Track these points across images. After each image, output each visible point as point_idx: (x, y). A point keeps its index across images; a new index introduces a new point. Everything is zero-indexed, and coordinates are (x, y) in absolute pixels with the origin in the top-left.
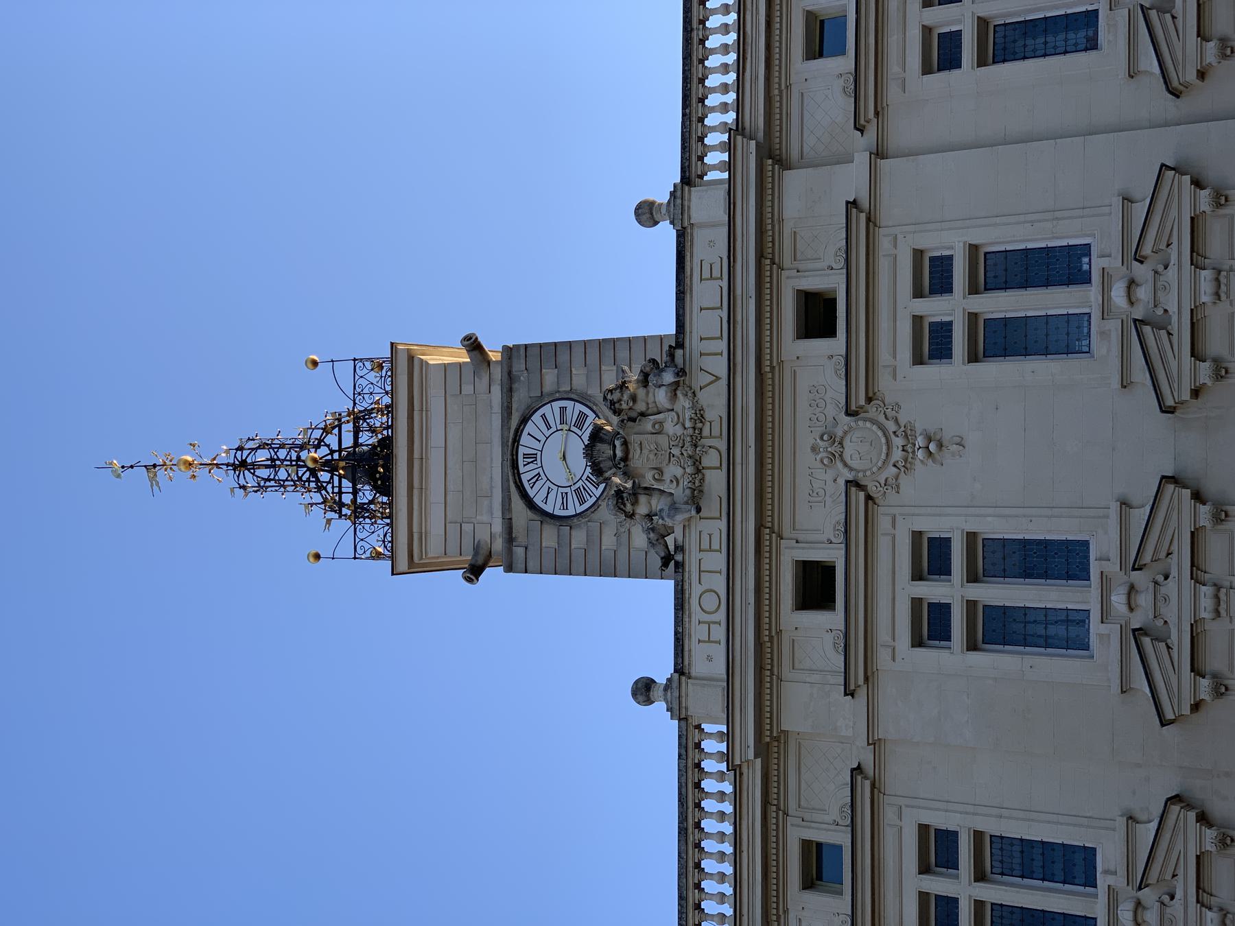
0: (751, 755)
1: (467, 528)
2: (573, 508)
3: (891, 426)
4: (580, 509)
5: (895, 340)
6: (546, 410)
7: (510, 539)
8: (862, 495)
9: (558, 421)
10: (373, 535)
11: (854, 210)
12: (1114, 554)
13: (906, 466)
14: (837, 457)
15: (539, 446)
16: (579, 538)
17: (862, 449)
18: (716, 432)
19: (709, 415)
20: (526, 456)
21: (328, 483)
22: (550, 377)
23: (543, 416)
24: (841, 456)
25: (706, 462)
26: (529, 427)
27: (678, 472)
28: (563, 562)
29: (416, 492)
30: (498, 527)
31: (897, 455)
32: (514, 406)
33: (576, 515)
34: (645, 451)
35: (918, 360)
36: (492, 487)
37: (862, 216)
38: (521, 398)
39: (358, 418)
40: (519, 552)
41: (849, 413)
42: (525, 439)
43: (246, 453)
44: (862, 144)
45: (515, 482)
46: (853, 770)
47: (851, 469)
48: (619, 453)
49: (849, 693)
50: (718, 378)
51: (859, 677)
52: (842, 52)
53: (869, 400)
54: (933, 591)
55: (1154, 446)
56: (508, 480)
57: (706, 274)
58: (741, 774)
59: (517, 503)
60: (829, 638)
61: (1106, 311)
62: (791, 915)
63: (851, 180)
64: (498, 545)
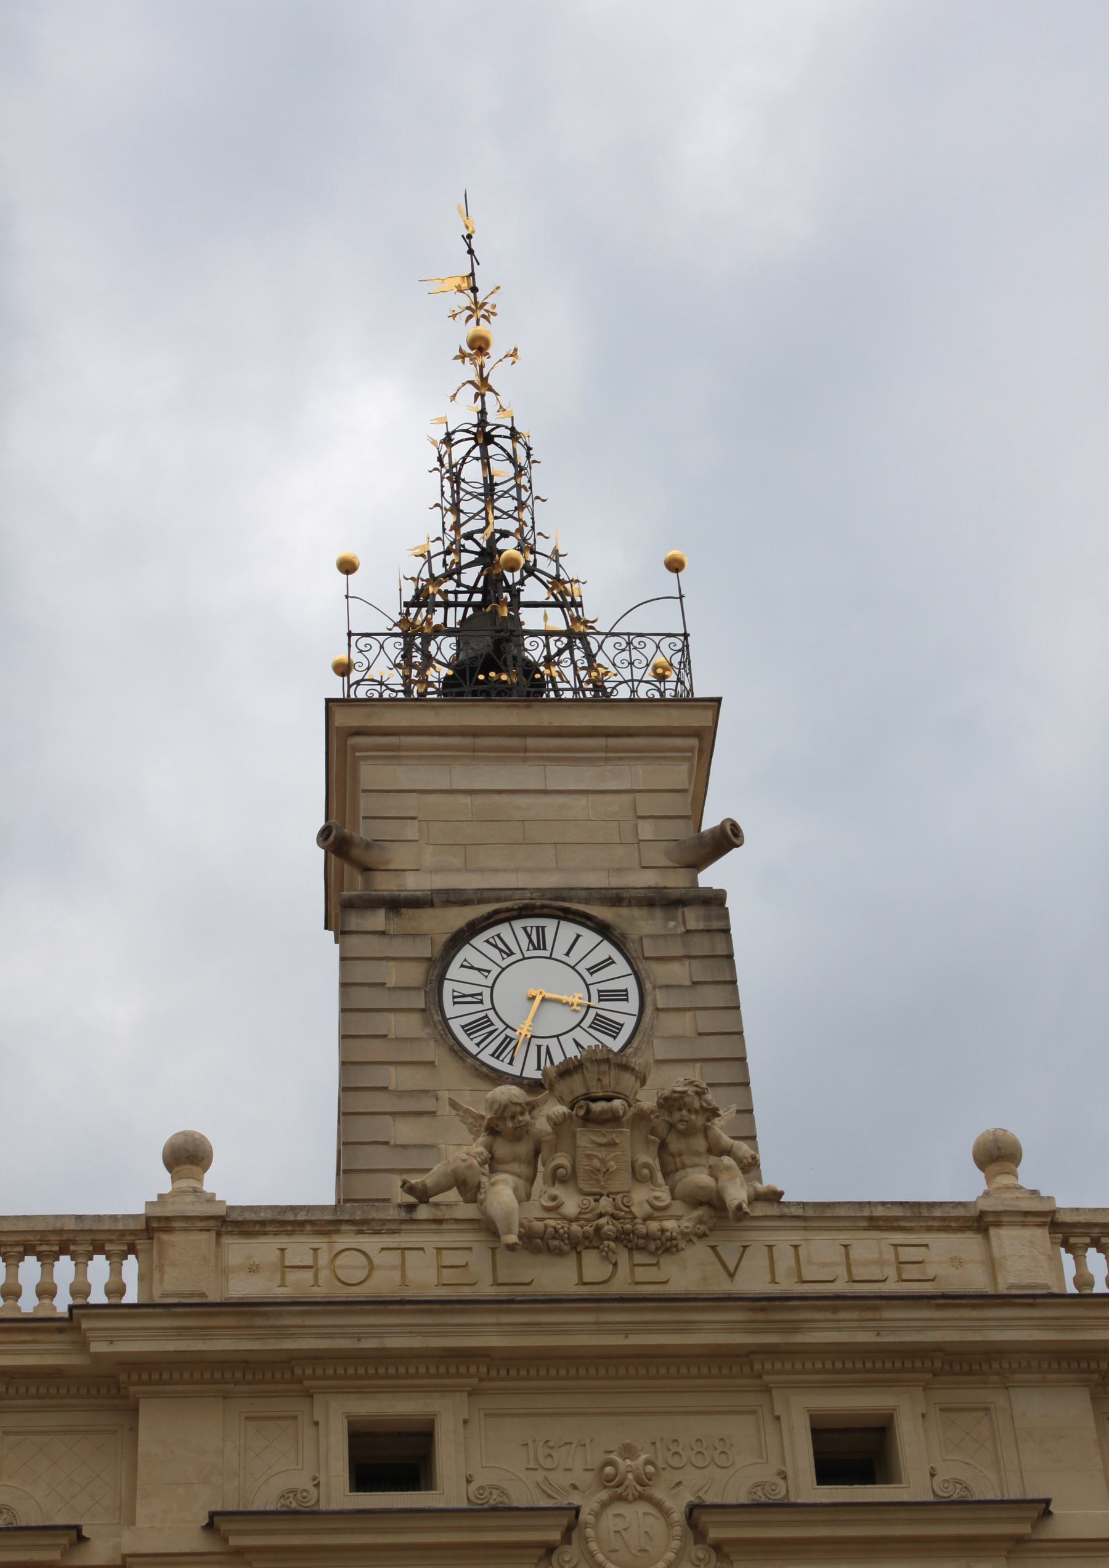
0: (97, 1347)
1: (411, 831)
2: (457, 1015)
4: (456, 1026)
6: (621, 966)
7: (395, 905)
8: (555, 1536)
9: (602, 986)
10: (383, 667)
11: (1034, 1514)
14: (618, 1490)
15: (559, 953)
16: (409, 1025)
18: (642, 1274)
19: (666, 1261)
20: (541, 931)
21: (459, 584)
22: (678, 973)
23: (610, 961)
24: (621, 1498)
25: (590, 1258)
26: (590, 938)
28: (363, 998)
29: (468, 741)
30: (414, 884)
32: (625, 911)
33: (445, 1020)
34: (602, 1153)
36: (482, 870)
38: (642, 924)
39: (577, 634)
40: (378, 920)
41: (693, 1511)
42: (569, 930)
43: (507, 444)
45: (496, 912)
46: (78, 1529)
47: (597, 1515)
48: (598, 1107)
49: (213, 1523)
50: (732, 1275)
53: (718, 1547)
56: (498, 900)
57: (906, 1254)
58: (61, 1331)
60: (302, 1481)
64: (385, 885)
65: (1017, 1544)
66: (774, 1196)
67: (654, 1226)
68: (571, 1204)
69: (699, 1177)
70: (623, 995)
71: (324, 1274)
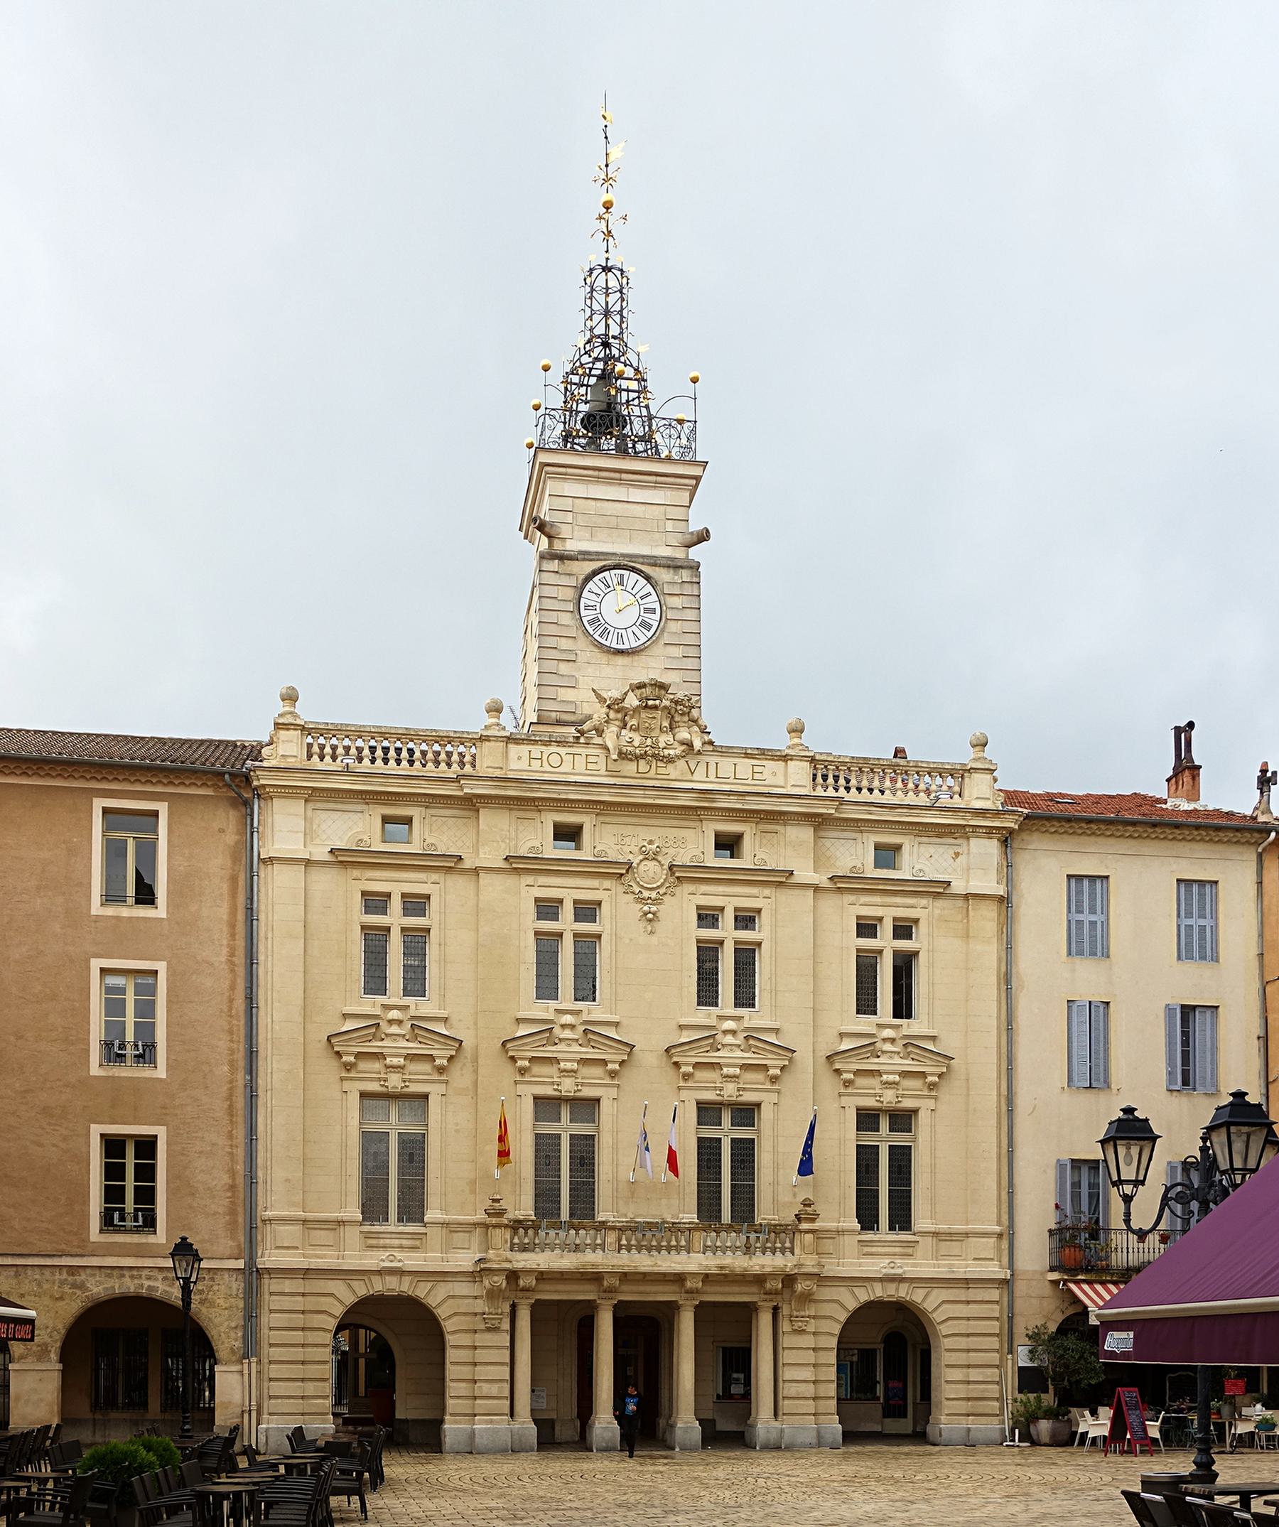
0: (466, 790)
3: (662, 891)
5: (712, 896)
12: (593, 1017)
13: (642, 900)
17: (651, 872)
18: (660, 771)
19: (670, 766)
25: (642, 762)
27: (636, 743)
29: (596, 473)
31: (646, 894)
35: (698, 908)
37: (781, 880)
41: (671, 867)
44: (822, 879)
51: (518, 865)
52: (877, 865)
53: (678, 878)
54: (568, 911)
55: (650, 1043)
57: (756, 769)
59: (590, 567)
61: (721, 1018)
62: (365, 807)
63: (805, 874)
65: (780, 884)
66: (711, 743)
67: (666, 752)
68: (638, 741)
69: (683, 734)
70: (654, 611)
71: (545, 763)
